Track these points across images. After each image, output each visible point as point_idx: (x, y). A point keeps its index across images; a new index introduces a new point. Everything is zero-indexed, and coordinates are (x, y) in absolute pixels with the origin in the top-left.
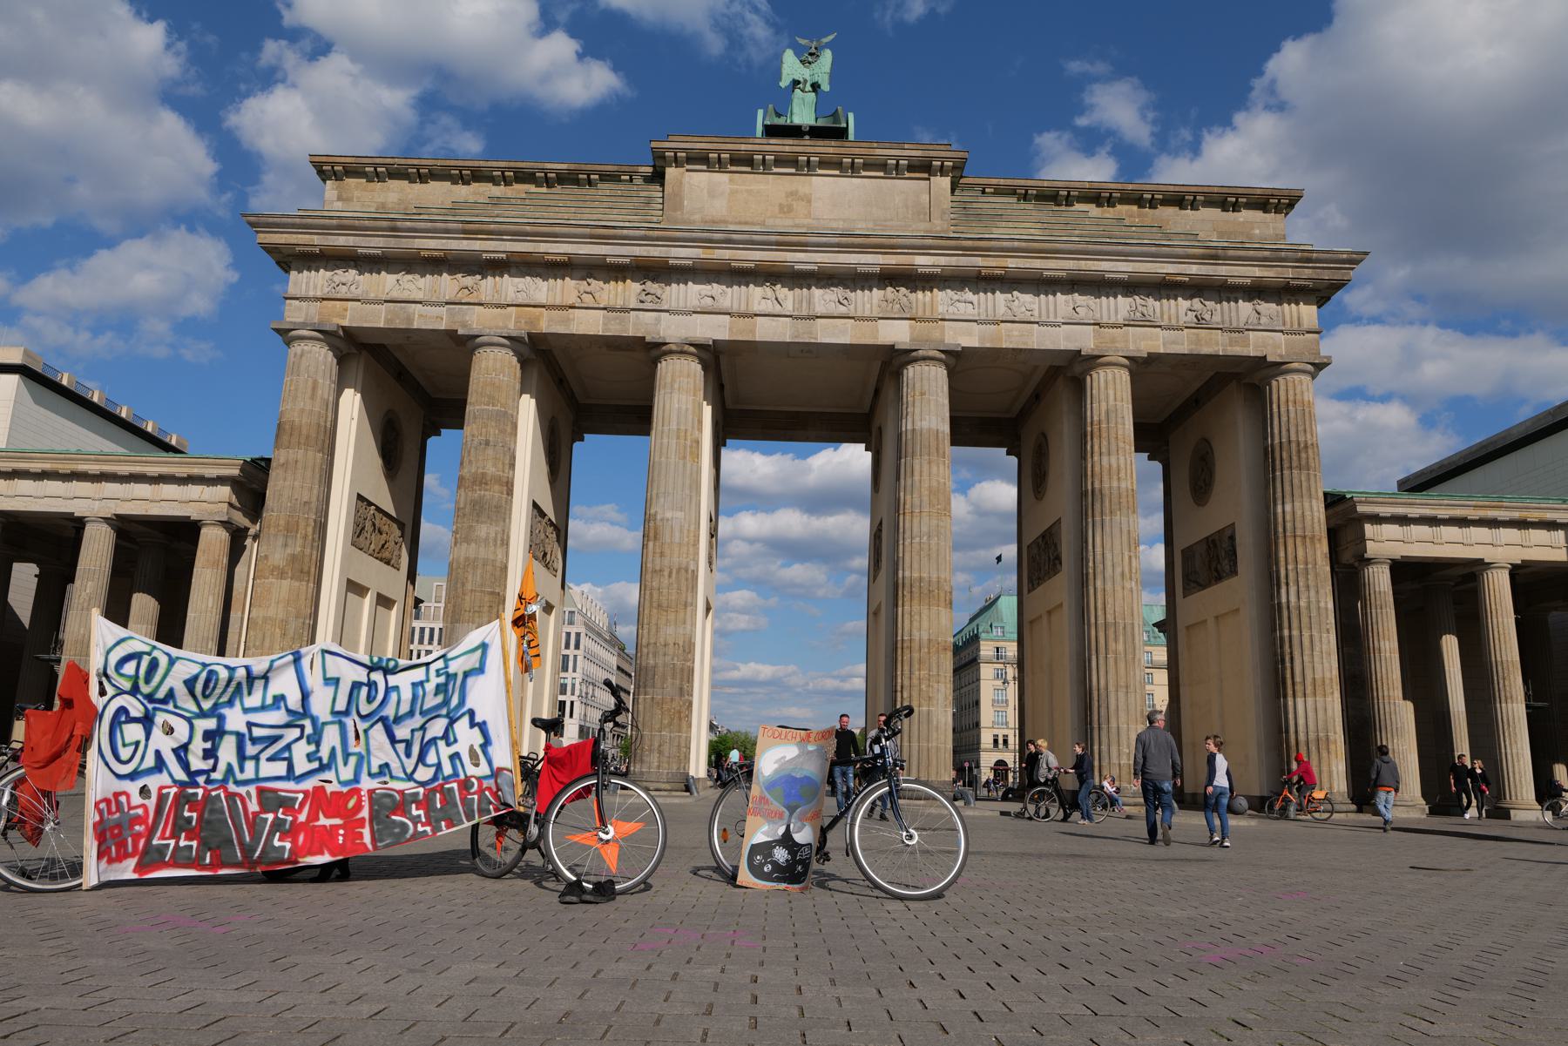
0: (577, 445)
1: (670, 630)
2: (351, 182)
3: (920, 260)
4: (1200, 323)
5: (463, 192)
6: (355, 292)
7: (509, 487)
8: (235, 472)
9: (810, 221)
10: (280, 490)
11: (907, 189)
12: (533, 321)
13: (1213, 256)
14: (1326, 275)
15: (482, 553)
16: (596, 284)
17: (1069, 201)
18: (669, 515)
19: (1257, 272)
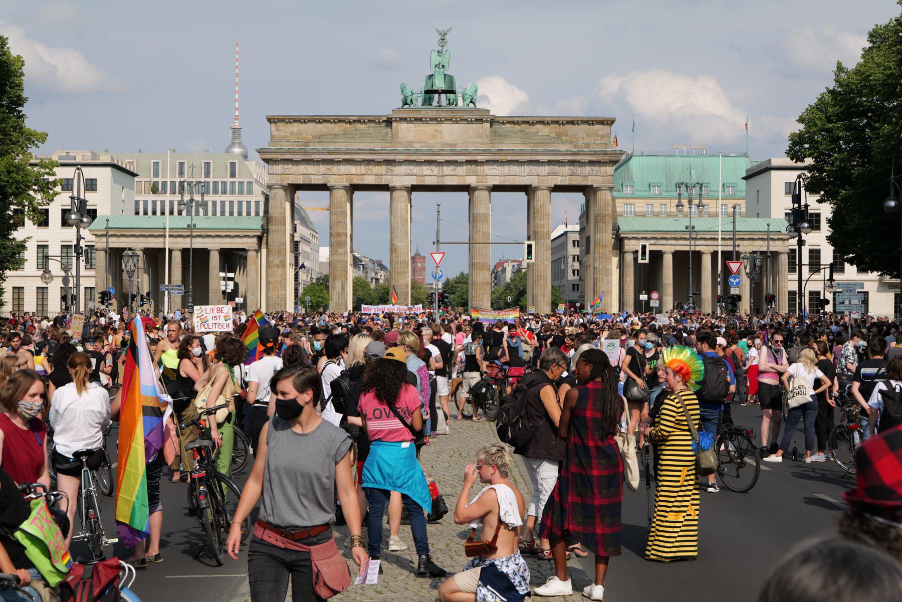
0: (354, 196)
1: (401, 281)
2: (280, 124)
3: (479, 158)
4: (573, 174)
5: (319, 126)
6: (291, 171)
7: (346, 235)
8: (259, 234)
9: (441, 141)
10: (273, 237)
11: (476, 126)
12: (351, 180)
13: (575, 154)
14: (613, 159)
15: (341, 258)
16: (371, 167)
17: (533, 124)
18: (399, 244)
19: (590, 158)
